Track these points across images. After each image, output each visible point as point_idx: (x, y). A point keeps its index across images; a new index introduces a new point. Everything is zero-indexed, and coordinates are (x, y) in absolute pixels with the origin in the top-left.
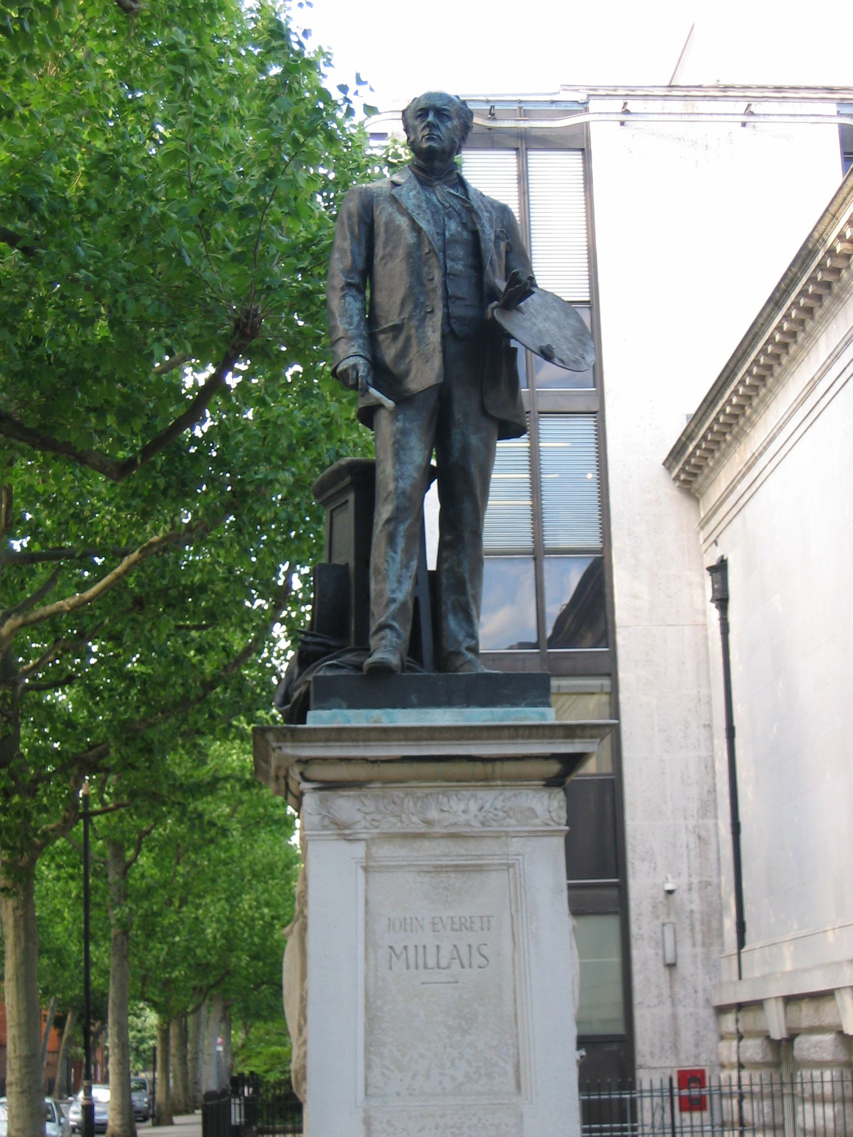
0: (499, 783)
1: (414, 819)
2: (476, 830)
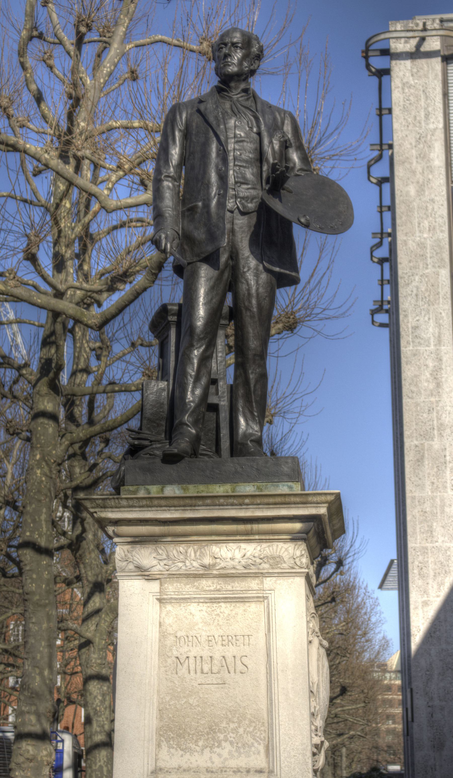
0: (257, 537)
1: (195, 564)
2: (240, 572)
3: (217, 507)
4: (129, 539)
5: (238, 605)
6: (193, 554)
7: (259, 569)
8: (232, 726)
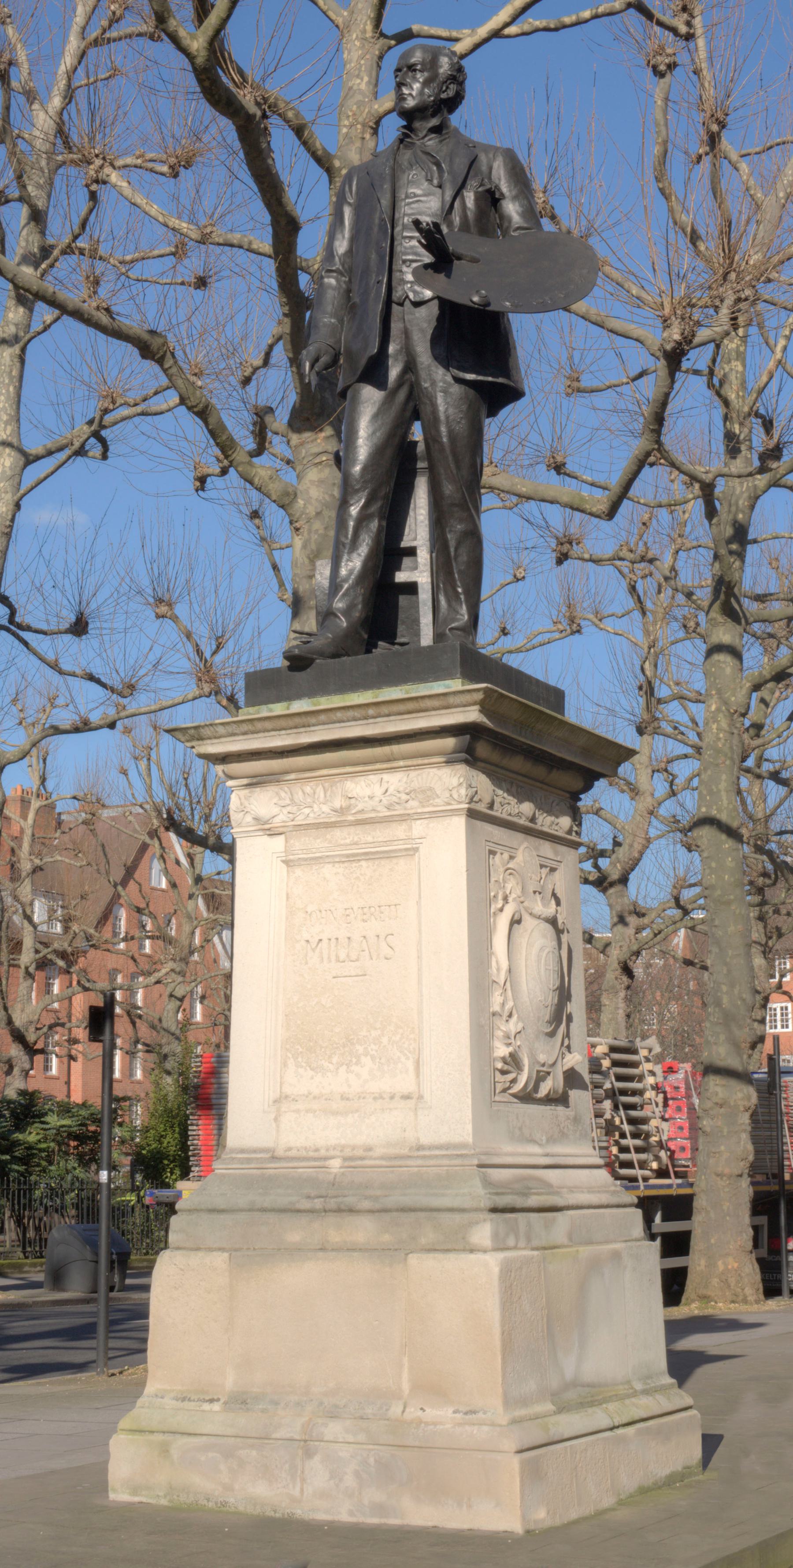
0: (401, 763)
1: (325, 808)
2: (381, 815)
3: (337, 725)
4: (245, 781)
5: (383, 862)
6: (322, 795)
7: (406, 809)
8: (374, 1033)
